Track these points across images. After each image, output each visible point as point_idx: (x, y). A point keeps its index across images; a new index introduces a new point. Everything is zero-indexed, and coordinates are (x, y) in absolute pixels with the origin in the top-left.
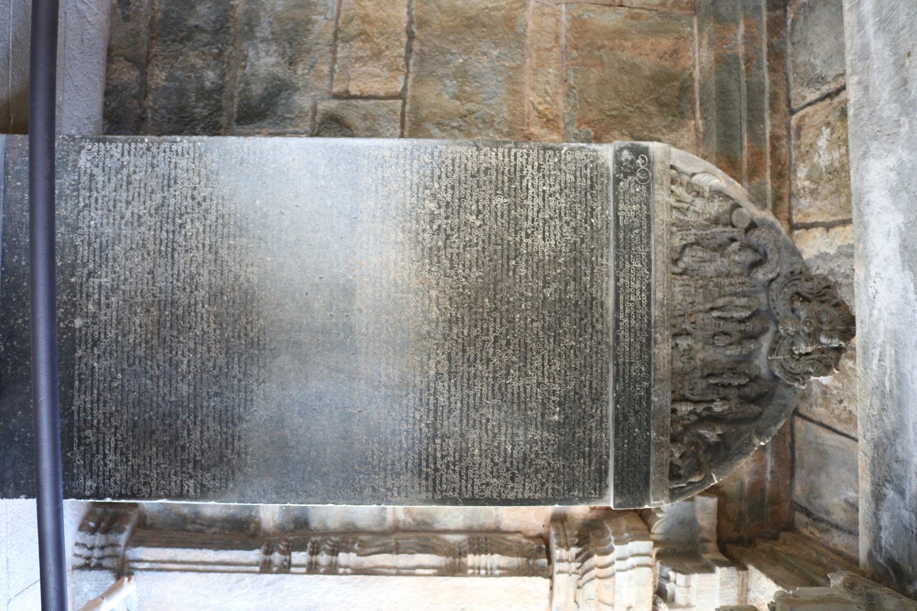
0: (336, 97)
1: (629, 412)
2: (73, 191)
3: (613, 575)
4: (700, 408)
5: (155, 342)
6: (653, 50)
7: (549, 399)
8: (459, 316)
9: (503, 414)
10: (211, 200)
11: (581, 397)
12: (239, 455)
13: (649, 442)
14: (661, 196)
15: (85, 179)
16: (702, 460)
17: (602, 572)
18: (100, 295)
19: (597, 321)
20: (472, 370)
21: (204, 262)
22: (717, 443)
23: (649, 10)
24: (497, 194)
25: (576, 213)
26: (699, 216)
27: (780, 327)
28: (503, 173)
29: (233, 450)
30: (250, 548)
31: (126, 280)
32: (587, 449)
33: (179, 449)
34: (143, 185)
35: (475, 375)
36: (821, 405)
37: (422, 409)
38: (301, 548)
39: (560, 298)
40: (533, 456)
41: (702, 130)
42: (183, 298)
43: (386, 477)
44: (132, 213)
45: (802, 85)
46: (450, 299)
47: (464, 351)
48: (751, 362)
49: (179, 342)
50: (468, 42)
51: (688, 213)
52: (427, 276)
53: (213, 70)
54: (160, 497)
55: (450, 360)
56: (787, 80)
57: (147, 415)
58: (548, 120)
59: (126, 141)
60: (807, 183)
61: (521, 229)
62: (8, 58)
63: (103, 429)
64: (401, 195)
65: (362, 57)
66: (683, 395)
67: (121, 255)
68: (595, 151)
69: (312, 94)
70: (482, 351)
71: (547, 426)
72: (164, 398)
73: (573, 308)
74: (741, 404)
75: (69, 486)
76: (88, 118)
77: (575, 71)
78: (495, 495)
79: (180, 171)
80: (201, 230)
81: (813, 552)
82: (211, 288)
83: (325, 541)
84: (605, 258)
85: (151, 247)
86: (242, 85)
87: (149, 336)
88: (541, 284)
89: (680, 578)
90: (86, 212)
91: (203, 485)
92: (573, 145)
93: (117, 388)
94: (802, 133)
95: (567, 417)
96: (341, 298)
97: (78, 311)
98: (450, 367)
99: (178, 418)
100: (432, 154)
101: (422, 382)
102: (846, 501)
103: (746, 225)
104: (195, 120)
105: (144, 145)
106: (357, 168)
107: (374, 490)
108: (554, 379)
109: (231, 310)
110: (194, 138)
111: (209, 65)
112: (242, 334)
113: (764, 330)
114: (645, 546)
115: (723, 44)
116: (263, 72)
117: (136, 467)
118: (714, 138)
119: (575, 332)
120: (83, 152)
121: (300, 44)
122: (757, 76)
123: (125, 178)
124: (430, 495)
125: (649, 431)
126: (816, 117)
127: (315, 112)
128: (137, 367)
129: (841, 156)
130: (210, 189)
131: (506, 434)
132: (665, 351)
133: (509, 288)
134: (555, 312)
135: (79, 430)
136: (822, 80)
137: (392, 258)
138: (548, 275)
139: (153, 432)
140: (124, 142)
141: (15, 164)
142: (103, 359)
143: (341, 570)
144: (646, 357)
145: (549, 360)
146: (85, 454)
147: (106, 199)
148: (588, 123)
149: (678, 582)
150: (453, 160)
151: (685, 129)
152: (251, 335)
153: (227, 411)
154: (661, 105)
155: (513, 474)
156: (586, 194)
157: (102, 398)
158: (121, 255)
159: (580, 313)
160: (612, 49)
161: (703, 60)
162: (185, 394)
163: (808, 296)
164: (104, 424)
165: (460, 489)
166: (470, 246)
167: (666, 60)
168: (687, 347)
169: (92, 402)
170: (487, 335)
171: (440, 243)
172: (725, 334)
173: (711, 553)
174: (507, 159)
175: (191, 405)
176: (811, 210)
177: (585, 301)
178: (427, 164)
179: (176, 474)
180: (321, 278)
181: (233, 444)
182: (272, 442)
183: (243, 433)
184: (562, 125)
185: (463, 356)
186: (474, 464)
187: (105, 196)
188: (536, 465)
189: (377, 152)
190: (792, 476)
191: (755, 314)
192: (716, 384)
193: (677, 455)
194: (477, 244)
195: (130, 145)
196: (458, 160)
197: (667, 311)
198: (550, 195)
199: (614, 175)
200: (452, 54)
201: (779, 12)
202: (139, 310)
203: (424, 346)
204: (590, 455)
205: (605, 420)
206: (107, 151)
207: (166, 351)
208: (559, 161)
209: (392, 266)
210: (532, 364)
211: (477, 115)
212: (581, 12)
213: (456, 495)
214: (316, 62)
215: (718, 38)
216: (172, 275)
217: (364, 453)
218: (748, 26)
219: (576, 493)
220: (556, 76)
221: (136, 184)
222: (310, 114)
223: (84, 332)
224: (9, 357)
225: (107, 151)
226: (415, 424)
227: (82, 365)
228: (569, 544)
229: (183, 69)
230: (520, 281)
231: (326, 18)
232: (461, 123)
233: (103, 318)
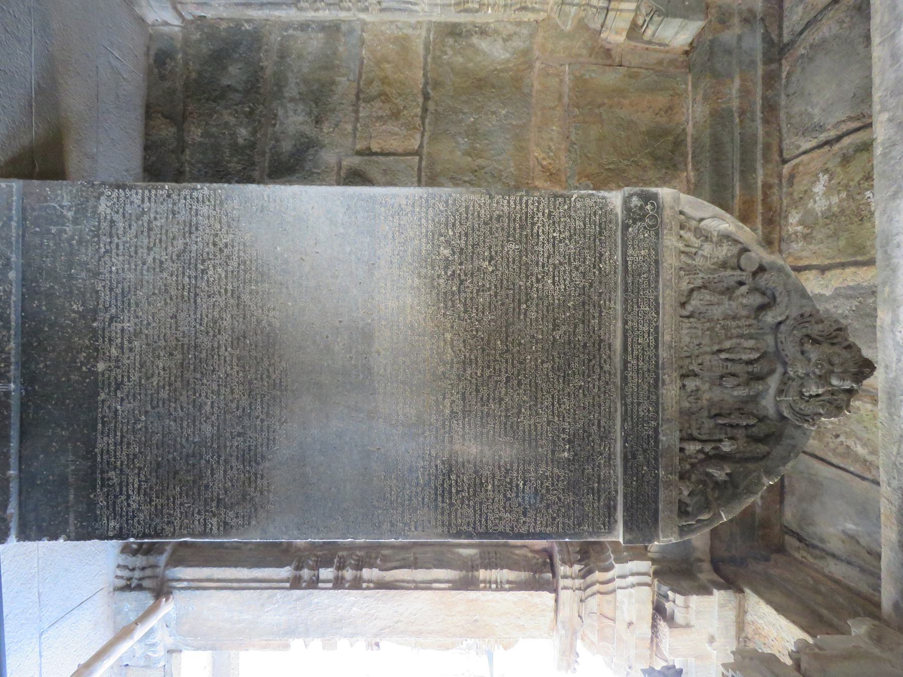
0: (359, 153)
1: (638, 451)
2: (93, 237)
3: (613, 591)
4: (708, 448)
5: (179, 384)
6: (650, 108)
7: (559, 436)
8: (472, 357)
9: (515, 451)
10: (233, 246)
11: (590, 435)
12: (262, 493)
13: (657, 482)
14: (670, 241)
15: (105, 225)
16: (710, 497)
17: (604, 588)
18: (122, 339)
19: (605, 361)
20: (485, 409)
21: (226, 307)
22: (725, 482)
23: (647, 69)
24: (508, 241)
25: (585, 258)
26: (707, 261)
27: (789, 369)
28: (514, 220)
29: (256, 488)
30: (281, 565)
32: (596, 485)
33: (202, 488)
34: (164, 231)
35: (488, 415)
36: (814, 439)
37: (438, 447)
38: (328, 564)
39: (569, 340)
40: (544, 491)
41: (693, 181)
42: (205, 341)
43: (403, 512)
44: (154, 259)
45: (797, 135)
46: (464, 341)
47: (477, 391)
48: (758, 403)
49: (202, 384)
50: (479, 102)
51: (695, 257)
52: (442, 319)
53: (246, 128)
54: (184, 536)
55: (464, 399)
56: (780, 131)
57: (171, 456)
58: (551, 174)
59: (146, 188)
60: (800, 228)
61: (532, 274)
62: (31, 106)
64: (417, 242)
65: (382, 117)
66: (691, 435)
68: (604, 198)
69: (337, 151)
70: (494, 390)
71: (558, 463)
72: (187, 439)
73: (581, 349)
74: (748, 443)
75: (92, 527)
76: (127, 171)
77: (576, 128)
78: (508, 530)
79: (201, 218)
80: (223, 276)
81: (809, 579)
82: (233, 332)
83: (350, 556)
84: (612, 302)
85: (173, 292)
86: (273, 142)
87: (173, 379)
88: (551, 327)
89: (680, 599)
90: (107, 258)
91: (226, 523)
92: (582, 192)
93: (140, 429)
94: (796, 180)
95: (576, 455)
96: (360, 341)
97: (101, 355)
98: (464, 406)
99: (202, 457)
100: (447, 202)
101: (437, 420)
102: (844, 532)
103: (754, 268)
104: (230, 174)
105: (165, 192)
106: (375, 216)
107: (392, 525)
108: (564, 417)
109: (253, 353)
110: (215, 185)
111: (241, 122)
112: (264, 376)
113: (772, 372)
114: (645, 566)
115: (718, 99)
116: (291, 130)
117: (159, 507)
118: (707, 187)
119: (584, 372)
120: (102, 198)
121: (325, 104)
122: (750, 127)
123: (146, 224)
124: (446, 529)
125: (658, 469)
126: (812, 165)
127: (340, 168)
128: (161, 409)
129: (840, 201)
130: (231, 236)
131: (518, 471)
132: (673, 392)
133: (520, 330)
134: (564, 354)
135: (102, 472)
136: (821, 128)
137: (409, 301)
138: (558, 318)
139: (176, 473)
140: (143, 189)
141: (33, 209)
142: (126, 401)
143: (364, 585)
144: (654, 397)
145: (559, 400)
146: (108, 495)
147: (128, 245)
148: (587, 176)
150: (467, 208)
151: (678, 180)
152: (274, 377)
153: (250, 450)
154: (656, 158)
155: (525, 508)
156: (595, 240)
159: (588, 354)
160: (611, 107)
161: (697, 115)
162: (209, 435)
163: (818, 338)
164: (127, 465)
165: (475, 523)
166: (483, 291)
167: (661, 116)
168: (694, 388)
169: (115, 444)
170: (499, 376)
171: (454, 288)
172: (733, 375)
173: (706, 574)
174: (518, 207)
175: (215, 446)
176: (804, 254)
177: (594, 344)
179: (199, 513)
180: (340, 322)
181: (256, 482)
184: (564, 179)
185: (477, 395)
186: (488, 499)
187: (127, 242)
188: (547, 500)
189: (393, 201)
190: (782, 502)
191: (764, 355)
192: (724, 425)
193: (686, 493)
194: (490, 289)
195: (150, 191)
196: (471, 208)
197: (675, 353)
198: (560, 242)
199: (623, 221)
200: (464, 113)
201: (774, 66)
202: (162, 354)
203: (439, 386)
204: (599, 491)
205: (613, 457)
206: (127, 198)
207: (190, 393)
208: (569, 208)
210: (542, 403)
211: (486, 170)
212: (582, 72)
213: (471, 529)
214: (341, 121)
215: (714, 93)
216: (195, 320)
218: (743, 80)
219: (586, 528)
220: (559, 133)
221: (157, 231)
222: (336, 169)
223: (107, 376)
224: (30, 400)
225: (127, 198)
226: (431, 461)
227: (105, 408)
228: (572, 560)
229: (217, 126)
230: (531, 324)
231: (349, 80)
232: (472, 177)
233: (126, 362)
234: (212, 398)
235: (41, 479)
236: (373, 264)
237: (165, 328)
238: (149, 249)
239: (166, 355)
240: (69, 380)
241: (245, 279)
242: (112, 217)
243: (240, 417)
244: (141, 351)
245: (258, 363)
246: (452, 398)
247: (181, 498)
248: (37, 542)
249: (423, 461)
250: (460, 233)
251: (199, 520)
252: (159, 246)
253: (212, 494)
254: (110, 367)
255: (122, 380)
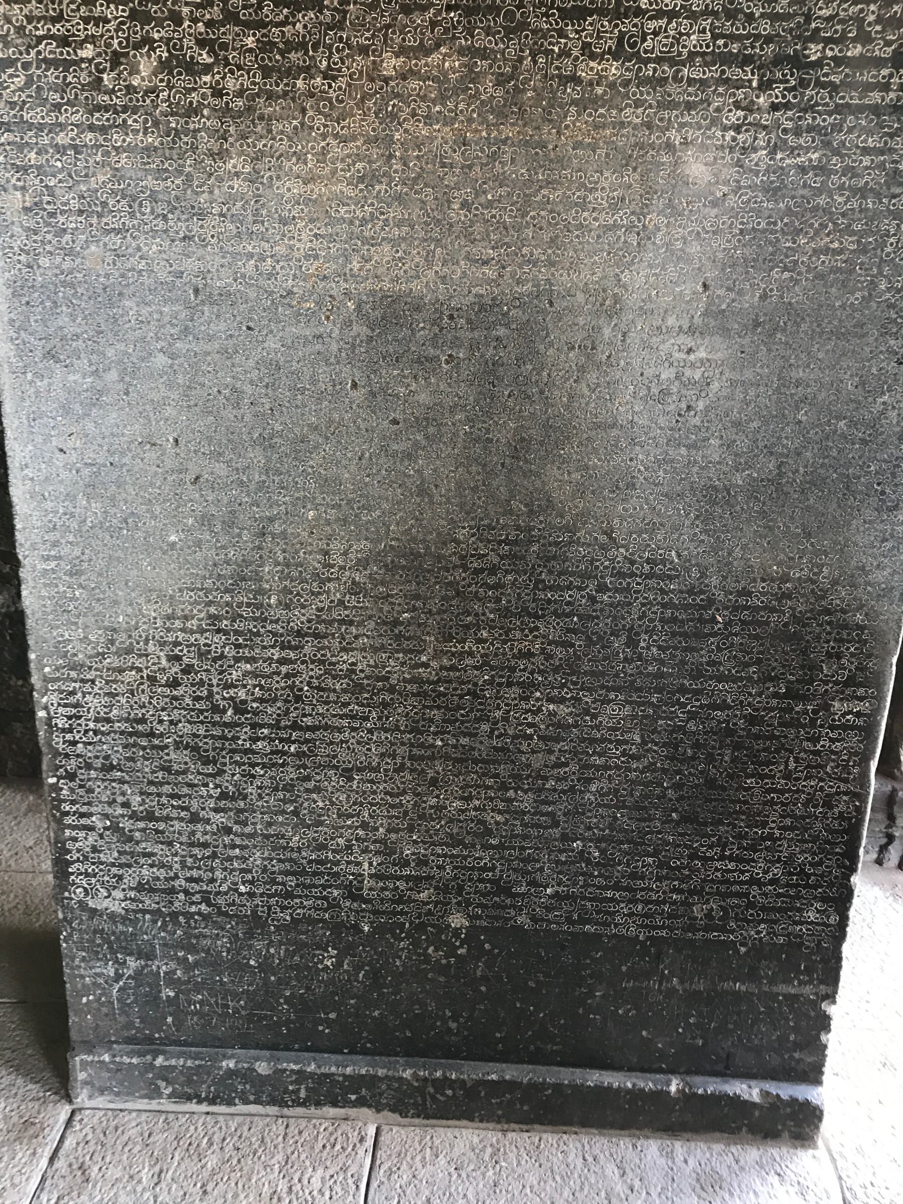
2: (177, 924)
15: (149, 902)
18: (399, 878)
21: (322, 662)
29: (773, 610)
31: (364, 826)
33: (755, 730)
34: (153, 789)
44: (216, 810)
49: (506, 719)
52: (342, 82)
54: (865, 775)
63: (693, 883)
67: (311, 834)
72: (633, 757)
79: (115, 712)
82: (382, 648)
85: (292, 774)
87: (490, 782)
90: (221, 901)
91: (850, 682)
93: (603, 852)
96: (406, 332)
101: (638, 104)
106: (64, 284)
109: (435, 604)
117: (788, 821)
123: (141, 825)
130: (151, 648)
135: (693, 928)
139: (711, 783)
140: (61, 827)
141: (130, 1025)
153: (674, 620)
157: (624, 882)
158: (311, 834)
164: (682, 881)
178: (29, 82)
179: (815, 740)
180: (355, 386)
181: (756, 609)
182: (763, 514)
183: (732, 585)
187: (183, 864)
189: (17, 229)
195: (67, 813)
203: (539, 96)
207: (524, 748)
209: (318, 189)
216: (354, 729)
217: (820, 276)
225: (86, 858)
226: (758, 125)
234: (538, 700)
235: (694, 1038)
236: (196, 291)
237: (374, 793)
238: (195, 819)
239: (437, 792)
240: (485, 979)
241: (255, 619)
242: (131, 889)
243: (589, 639)
244: (424, 843)
245: (458, 594)
246: (575, 52)
247: (773, 777)
248: (828, 1052)
249: (755, 150)
250: (86, 21)
251: (832, 740)
252: (187, 799)
253: (772, 709)
254: (459, 904)
255: (489, 881)
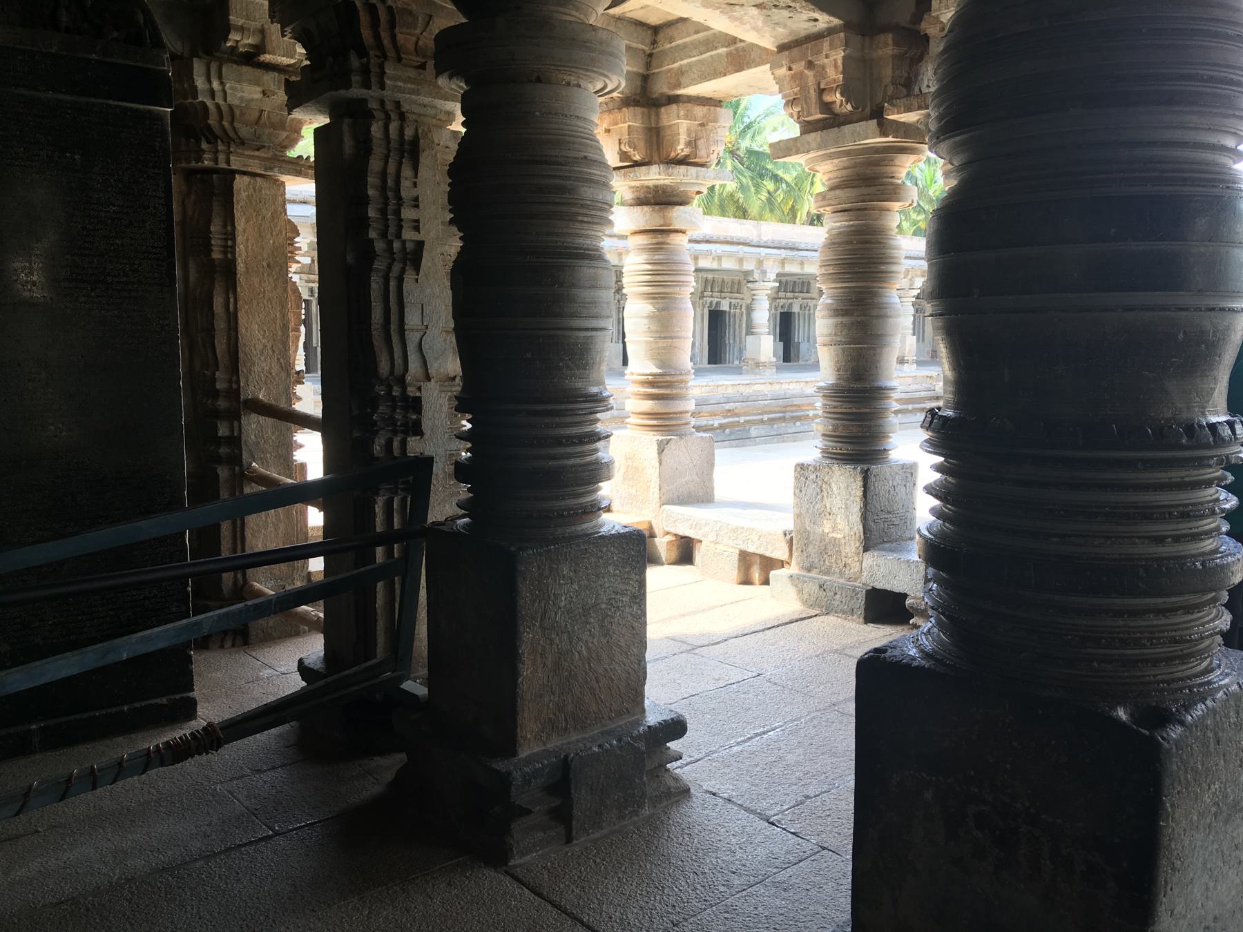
89: (234, 36)
143: (234, 386)
149: (238, 39)
193: (116, 34)
